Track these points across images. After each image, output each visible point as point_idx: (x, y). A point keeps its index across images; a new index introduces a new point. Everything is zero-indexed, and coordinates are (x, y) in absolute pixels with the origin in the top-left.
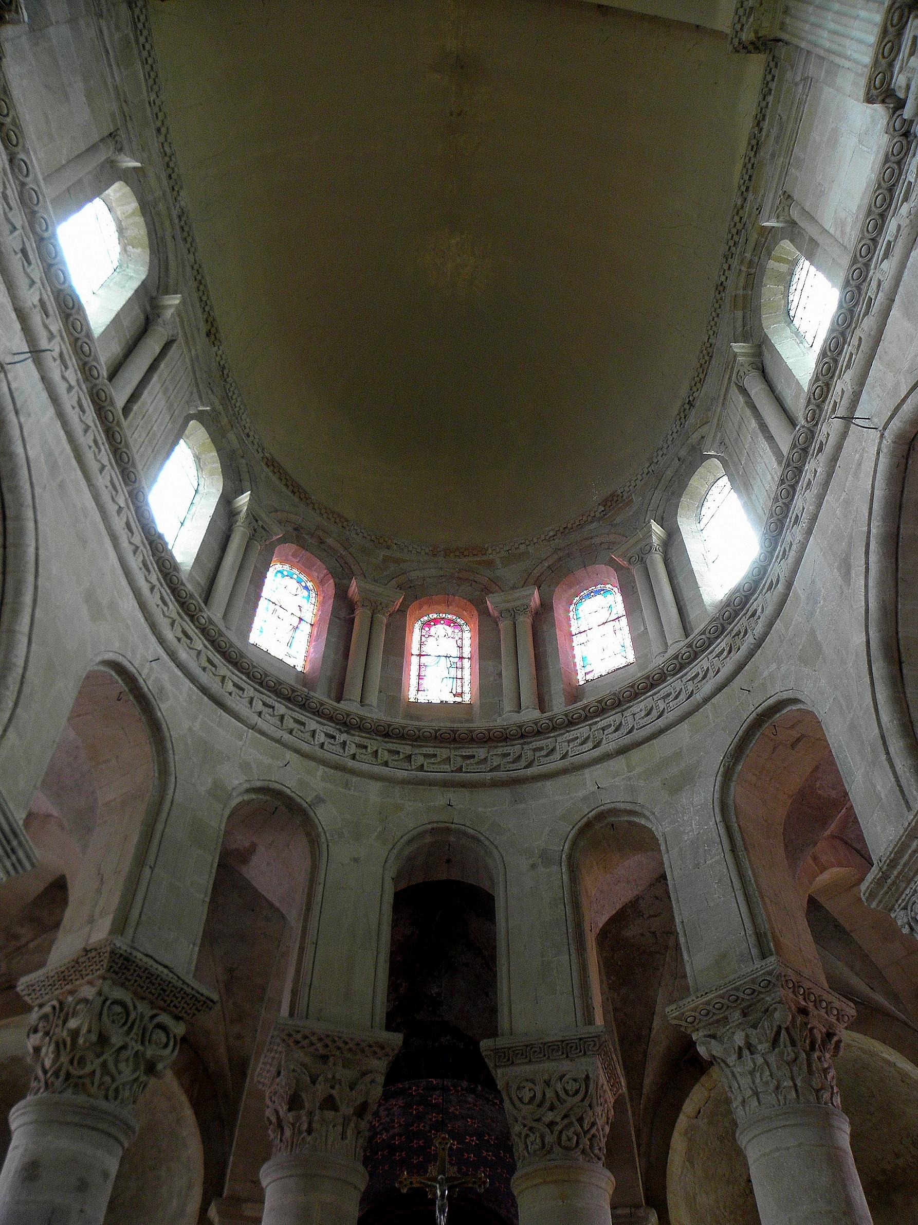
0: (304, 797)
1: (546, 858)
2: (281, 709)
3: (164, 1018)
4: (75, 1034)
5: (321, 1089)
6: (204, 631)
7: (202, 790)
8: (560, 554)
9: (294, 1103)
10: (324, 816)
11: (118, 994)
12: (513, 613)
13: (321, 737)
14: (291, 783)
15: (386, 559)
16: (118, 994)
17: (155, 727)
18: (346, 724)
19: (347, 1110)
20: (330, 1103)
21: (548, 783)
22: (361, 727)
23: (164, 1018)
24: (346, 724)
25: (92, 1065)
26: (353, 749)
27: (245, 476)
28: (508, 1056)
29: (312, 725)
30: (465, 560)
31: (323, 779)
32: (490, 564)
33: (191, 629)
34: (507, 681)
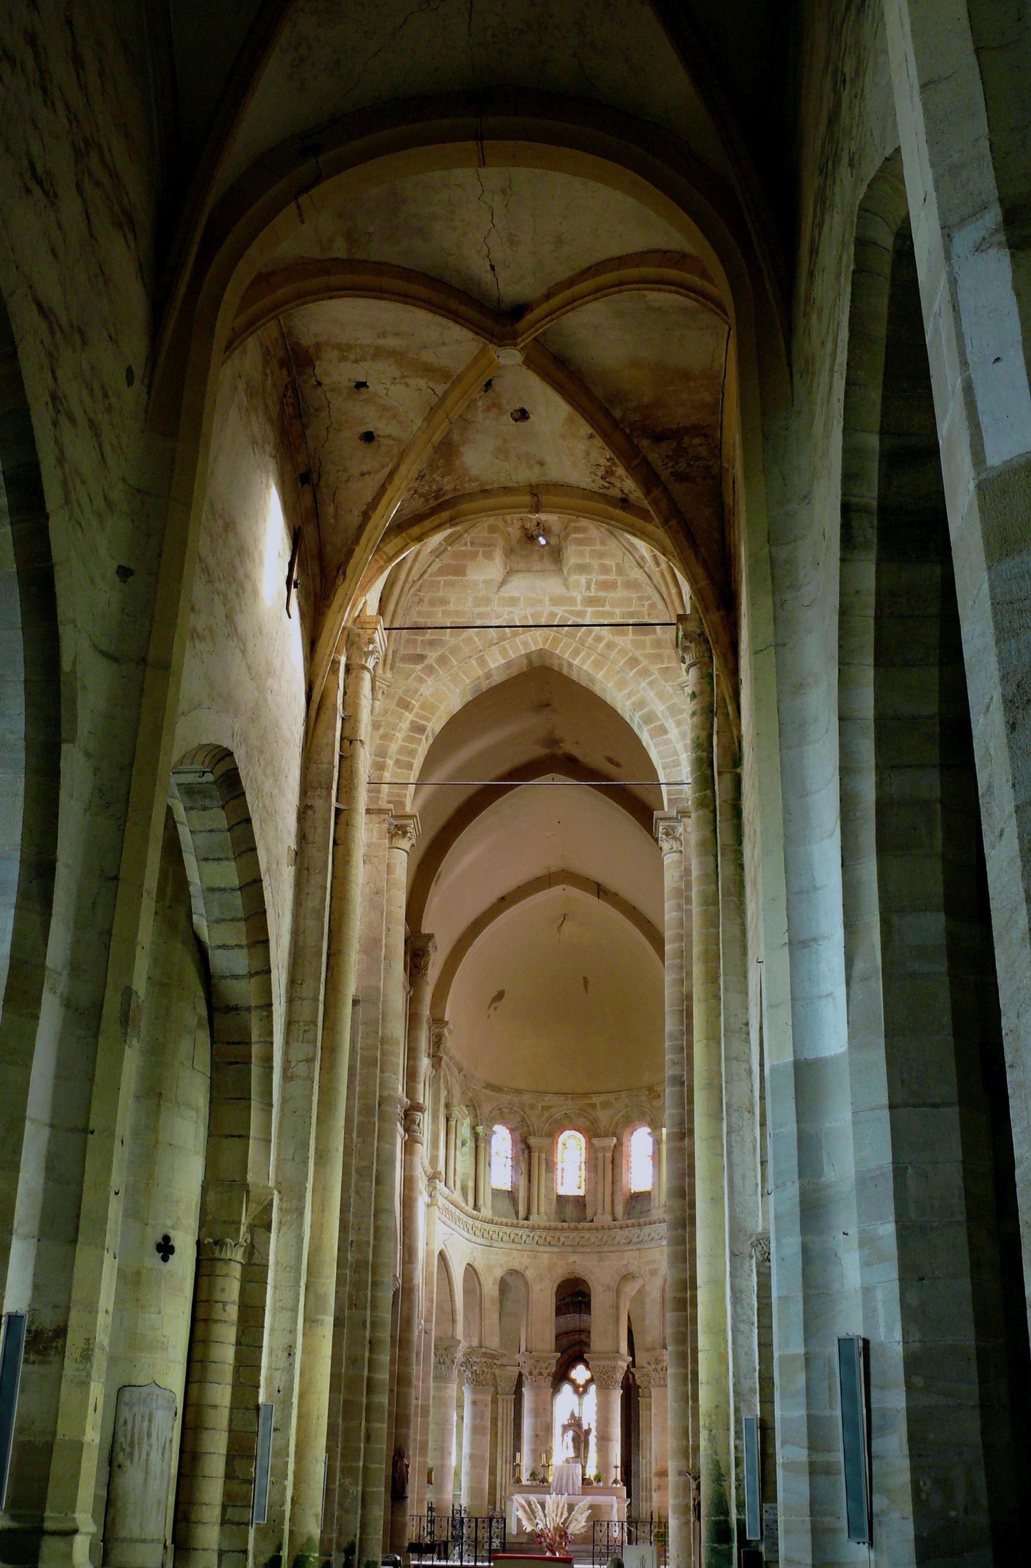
0: (520, 1268)
1: (609, 1288)
2: (508, 1230)
3: (496, 1361)
4: (476, 1371)
5: (538, 1370)
6: (481, 1221)
7: (491, 1284)
8: (628, 1109)
9: (531, 1374)
10: (530, 1274)
11: (484, 1360)
12: (604, 1149)
13: (524, 1237)
14: (517, 1264)
15: (544, 1108)
16: (484, 1360)
17: (475, 1270)
18: (533, 1228)
19: (545, 1375)
20: (541, 1374)
21: (612, 1254)
22: (539, 1228)
23: (496, 1361)
24: (533, 1228)
25: (482, 1378)
26: (536, 1238)
27: (477, 1108)
28: (593, 1359)
29: (520, 1232)
30: (582, 1102)
31: (528, 1258)
32: (593, 1106)
33: (478, 1223)
34: (600, 1189)
